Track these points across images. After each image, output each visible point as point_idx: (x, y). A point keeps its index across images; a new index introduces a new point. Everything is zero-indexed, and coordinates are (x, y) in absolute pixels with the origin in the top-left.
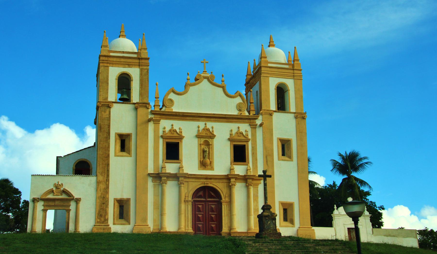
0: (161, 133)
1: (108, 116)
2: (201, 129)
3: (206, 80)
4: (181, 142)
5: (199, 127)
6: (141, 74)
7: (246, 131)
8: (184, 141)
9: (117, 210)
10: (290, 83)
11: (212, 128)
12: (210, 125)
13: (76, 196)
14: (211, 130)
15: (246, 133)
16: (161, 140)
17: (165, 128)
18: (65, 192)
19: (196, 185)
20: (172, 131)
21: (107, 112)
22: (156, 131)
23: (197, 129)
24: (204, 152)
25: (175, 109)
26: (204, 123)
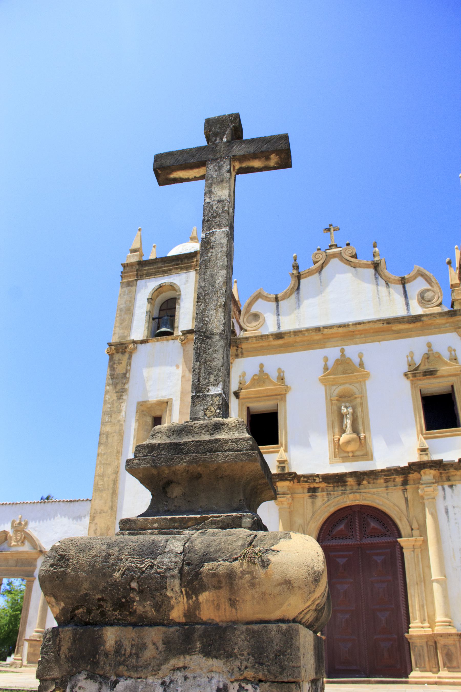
2: (331, 363)
3: (335, 262)
5: (326, 359)
8: (289, 397)
11: (361, 356)
15: (451, 353)
17: (244, 374)
26: (339, 348)
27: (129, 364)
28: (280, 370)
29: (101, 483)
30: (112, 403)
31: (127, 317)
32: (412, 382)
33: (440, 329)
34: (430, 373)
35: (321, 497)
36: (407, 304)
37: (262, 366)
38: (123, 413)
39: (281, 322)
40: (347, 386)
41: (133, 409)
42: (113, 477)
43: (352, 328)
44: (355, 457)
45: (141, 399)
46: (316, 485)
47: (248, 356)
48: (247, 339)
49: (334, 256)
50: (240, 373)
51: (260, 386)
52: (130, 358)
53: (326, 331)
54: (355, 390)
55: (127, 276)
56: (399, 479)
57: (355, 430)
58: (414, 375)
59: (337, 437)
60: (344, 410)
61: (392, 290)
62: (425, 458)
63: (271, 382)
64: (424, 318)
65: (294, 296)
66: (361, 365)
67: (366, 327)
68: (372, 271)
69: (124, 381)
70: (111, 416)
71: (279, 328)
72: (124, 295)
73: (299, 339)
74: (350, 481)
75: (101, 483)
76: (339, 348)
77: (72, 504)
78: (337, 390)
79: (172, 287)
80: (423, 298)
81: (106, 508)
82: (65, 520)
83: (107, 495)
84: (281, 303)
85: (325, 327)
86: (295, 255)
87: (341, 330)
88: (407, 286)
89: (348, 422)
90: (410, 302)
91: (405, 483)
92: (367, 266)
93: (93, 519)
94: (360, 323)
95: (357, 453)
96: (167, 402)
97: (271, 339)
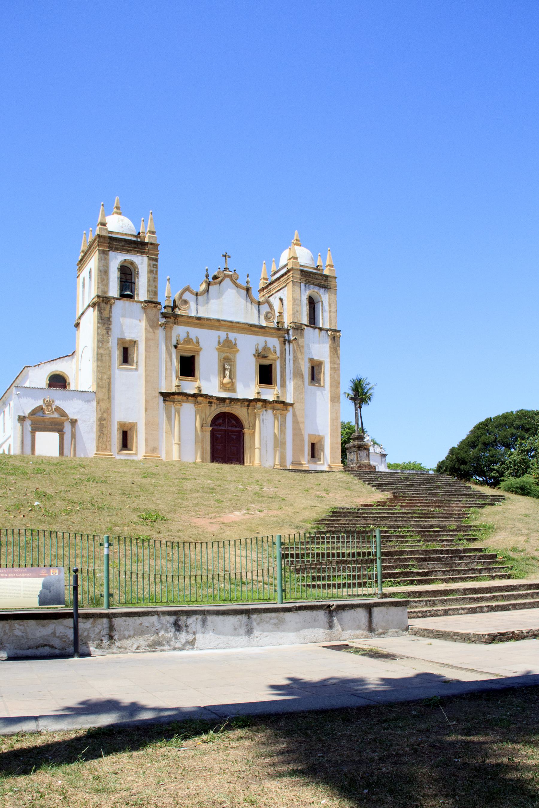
0: (174, 342)
1: (108, 316)
2: (222, 340)
4: (198, 354)
5: (219, 337)
6: (149, 265)
7: (274, 347)
11: (235, 339)
12: (232, 336)
13: (71, 416)
14: (234, 342)
16: (174, 350)
17: (178, 336)
18: (58, 409)
19: (216, 410)
20: (188, 340)
21: (107, 311)
22: (168, 338)
23: (217, 339)
26: (225, 333)
27: (110, 312)
28: (197, 338)
29: (101, 383)
30: (103, 335)
31: (105, 277)
32: (256, 359)
33: (271, 335)
34: (265, 357)
35: (214, 407)
36: (259, 317)
37: (188, 333)
38: (110, 343)
39: (198, 309)
40: (228, 354)
41: (116, 342)
42: (108, 380)
43: (234, 324)
44: (229, 390)
45: (120, 337)
46: (212, 401)
47: (181, 325)
48: (183, 316)
49: (228, 276)
50: (176, 334)
51: (188, 345)
52: (111, 308)
53: (222, 322)
54: (231, 357)
55: (102, 246)
56: (246, 404)
57: (230, 378)
58: (258, 356)
59: (222, 379)
60: (227, 367)
61: (253, 307)
62: (259, 397)
63: (194, 344)
64: (267, 328)
65: (205, 295)
66: (235, 344)
67: (241, 325)
68: (245, 292)
69: (109, 323)
70: (103, 344)
71: (197, 313)
72: (102, 260)
73: (208, 322)
74: (228, 401)
75: (101, 383)
76: (225, 333)
77: (83, 393)
78: (224, 355)
79: (132, 263)
80: (267, 316)
81: (106, 398)
82: (80, 402)
83: (105, 390)
84: (199, 297)
85: (222, 320)
86: (207, 268)
87: (229, 324)
88: (260, 306)
89: (227, 373)
90: (261, 316)
91: (248, 406)
92: (243, 288)
93: (98, 403)
94: (238, 323)
95: (230, 389)
96: (135, 342)
97: (195, 319)
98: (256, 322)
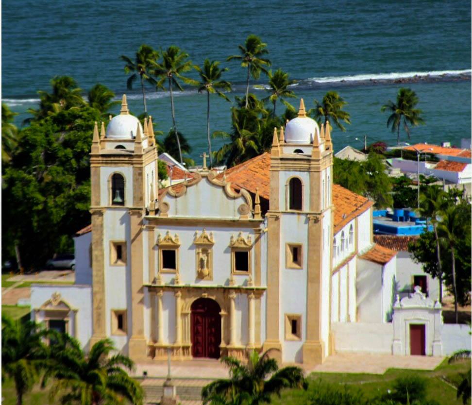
1: (101, 223)
3: (204, 180)
6: (134, 174)
8: (180, 249)
9: (115, 322)
10: (304, 177)
12: (207, 233)
14: (209, 238)
17: (159, 236)
18: (61, 303)
22: (150, 239)
24: (202, 261)
25: (171, 215)
98: (230, 218)
